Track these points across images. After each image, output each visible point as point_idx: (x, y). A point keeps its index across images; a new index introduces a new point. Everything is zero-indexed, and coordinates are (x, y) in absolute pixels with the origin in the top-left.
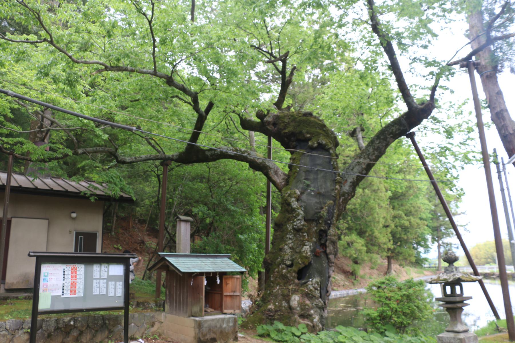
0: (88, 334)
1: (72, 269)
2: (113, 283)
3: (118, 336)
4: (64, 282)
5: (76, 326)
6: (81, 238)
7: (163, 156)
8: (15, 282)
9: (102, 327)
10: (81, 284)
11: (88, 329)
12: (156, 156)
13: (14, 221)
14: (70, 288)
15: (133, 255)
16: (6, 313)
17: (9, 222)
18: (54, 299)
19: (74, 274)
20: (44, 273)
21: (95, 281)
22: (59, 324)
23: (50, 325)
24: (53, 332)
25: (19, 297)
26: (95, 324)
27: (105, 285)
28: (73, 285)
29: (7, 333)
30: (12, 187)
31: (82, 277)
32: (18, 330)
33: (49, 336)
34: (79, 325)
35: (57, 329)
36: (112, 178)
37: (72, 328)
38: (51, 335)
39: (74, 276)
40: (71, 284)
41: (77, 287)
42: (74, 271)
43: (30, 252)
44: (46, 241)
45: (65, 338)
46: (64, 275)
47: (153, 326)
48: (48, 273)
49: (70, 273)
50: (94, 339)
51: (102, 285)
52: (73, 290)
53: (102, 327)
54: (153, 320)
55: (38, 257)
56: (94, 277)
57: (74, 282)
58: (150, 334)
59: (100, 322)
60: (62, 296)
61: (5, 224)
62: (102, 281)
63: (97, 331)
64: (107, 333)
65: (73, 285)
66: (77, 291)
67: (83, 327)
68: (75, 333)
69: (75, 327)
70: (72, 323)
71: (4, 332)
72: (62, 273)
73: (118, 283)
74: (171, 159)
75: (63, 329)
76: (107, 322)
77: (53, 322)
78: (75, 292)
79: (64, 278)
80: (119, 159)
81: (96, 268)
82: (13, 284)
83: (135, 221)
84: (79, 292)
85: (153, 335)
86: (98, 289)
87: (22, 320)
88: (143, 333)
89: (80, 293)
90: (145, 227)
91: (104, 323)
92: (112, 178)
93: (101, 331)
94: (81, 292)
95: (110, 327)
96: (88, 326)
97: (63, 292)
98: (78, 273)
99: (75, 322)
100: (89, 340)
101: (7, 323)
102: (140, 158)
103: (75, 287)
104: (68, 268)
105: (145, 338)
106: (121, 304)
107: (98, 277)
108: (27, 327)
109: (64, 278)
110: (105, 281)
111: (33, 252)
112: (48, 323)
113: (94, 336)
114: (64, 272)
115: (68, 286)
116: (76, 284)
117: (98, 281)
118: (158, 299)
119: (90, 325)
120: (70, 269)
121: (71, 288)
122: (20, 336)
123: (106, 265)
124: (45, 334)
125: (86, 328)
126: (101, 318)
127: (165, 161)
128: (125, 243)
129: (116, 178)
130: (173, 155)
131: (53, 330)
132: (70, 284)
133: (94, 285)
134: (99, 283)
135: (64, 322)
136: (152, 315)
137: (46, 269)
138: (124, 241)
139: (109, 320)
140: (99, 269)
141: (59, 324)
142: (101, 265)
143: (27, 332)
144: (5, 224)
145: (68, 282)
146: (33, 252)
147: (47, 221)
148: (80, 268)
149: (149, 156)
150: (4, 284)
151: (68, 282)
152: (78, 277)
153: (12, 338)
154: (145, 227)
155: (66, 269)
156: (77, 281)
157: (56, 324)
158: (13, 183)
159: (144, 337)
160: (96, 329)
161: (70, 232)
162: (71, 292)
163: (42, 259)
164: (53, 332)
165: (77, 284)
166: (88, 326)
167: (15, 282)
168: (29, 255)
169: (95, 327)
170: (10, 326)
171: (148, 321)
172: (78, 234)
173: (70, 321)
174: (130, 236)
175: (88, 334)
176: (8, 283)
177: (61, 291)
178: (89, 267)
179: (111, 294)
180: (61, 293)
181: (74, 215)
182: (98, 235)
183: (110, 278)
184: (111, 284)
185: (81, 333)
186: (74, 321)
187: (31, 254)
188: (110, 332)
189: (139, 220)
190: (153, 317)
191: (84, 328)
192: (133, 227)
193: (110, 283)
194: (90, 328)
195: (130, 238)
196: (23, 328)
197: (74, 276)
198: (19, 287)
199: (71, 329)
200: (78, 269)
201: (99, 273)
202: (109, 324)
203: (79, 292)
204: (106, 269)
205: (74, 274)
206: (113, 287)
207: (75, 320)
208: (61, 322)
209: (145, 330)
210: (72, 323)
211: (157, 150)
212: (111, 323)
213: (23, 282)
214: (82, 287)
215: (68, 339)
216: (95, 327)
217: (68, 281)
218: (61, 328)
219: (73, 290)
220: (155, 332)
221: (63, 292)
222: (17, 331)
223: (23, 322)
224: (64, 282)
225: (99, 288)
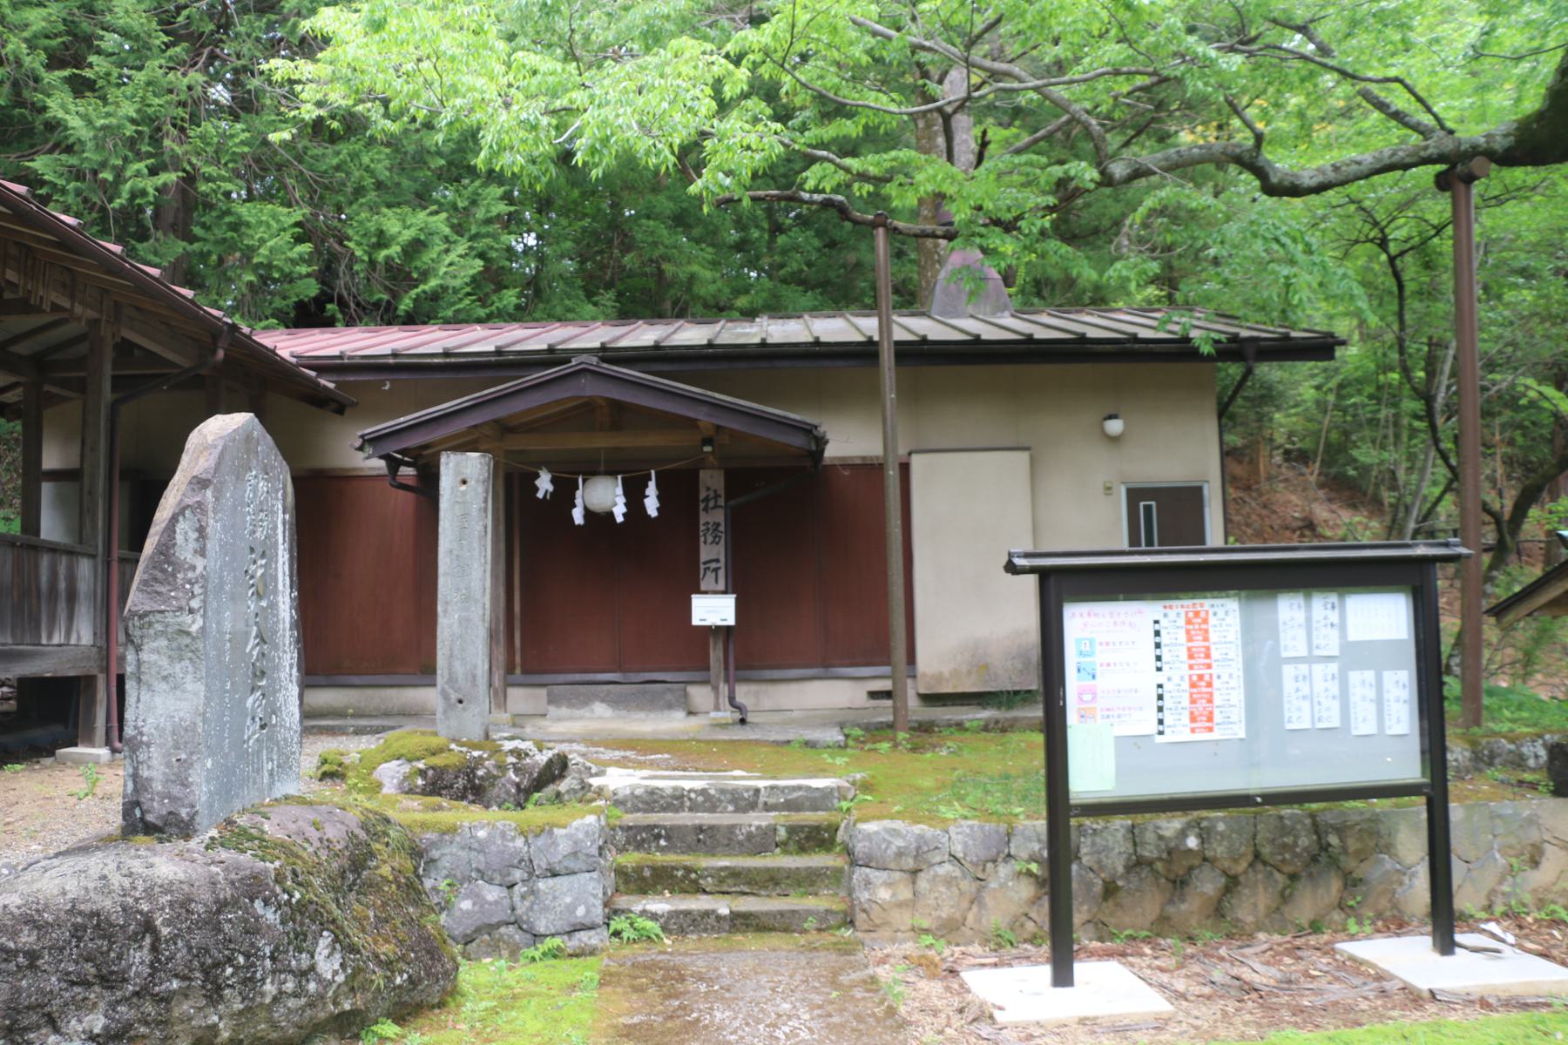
0: (1261, 889)
1: (1189, 622)
2: (1369, 675)
3: (1383, 903)
4: (1160, 678)
5: (1209, 854)
6: (1148, 509)
7: (1448, 145)
8: (946, 674)
9: (1314, 859)
10: (1233, 683)
11: (1260, 867)
12: (1418, 148)
13: (917, 462)
14: (1186, 702)
15: (1447, 545)
16: (941, 786)
17: (905, 469)
18: (1129, 746)
19: (1198, 643)
20: (1078, 641)
21: (1288, 671)
22: (1144, 843)
23: (1107, 849)
24: (1121, 877)
25: (967, 725)
26: (1284, 846)
27: (1335, 688)
28: (1201, 687)
29: (958, 873)
30: (897, 343)
31: (1235, 653)
32: (994, 861)
33: (1110, 890)
34: (1219, 850)
35: (1137, 864)
36: (1277, 240)
37: (1196, 862)
38: (1117, 888)
39: (1200, 655)
40: (1193, 685)
41: (1217, 700)
42: (1197, 628)
43: (1010, 555)
44: (1029, 526)
45: (1171, 901)
46: (1158, 645)
47: (1535, 863)
48: (1091, 642)
49: (1182, 636)
50: (1286, 909)
51: (1319, 685)
52: (1203, 717)
53: (1314, 859)
54: (1534, 835)
55: (1044, 574)
56: (1284, 654)
57: (1201, 677)
58: (1528, 898)
59: (1304, 841)
60: (1159, 739)
61: (892, 473)
62: (1318, 668)
63: (1293, 877)
64: (1335, 885)
65: (1201, 687)
66: (1217, 718)
67: (1236, 861)
68: (1208, 885)
69: (1205, 859)
70: (1192, 842)
71: (948, 867)
72: (1152, 640)
73: (1389, 677)
74: (1475, 152)
75: (1159, 866)
76: (1333, 840)
77: (1119, 835)
78: (1210, 719)
79: (1159, 658)
80: (1274, 180)
81: (1289, 610)
82: (939, 678)
83: (1271, 457)
84: (1228, 721)
85: (1541, 904)
86: (1306, 705)
87: (1003, 827)
88: (1493, 892)
89: (1232, 724)
90: (1312, 473)
91: (1325, 848)
92: (1277, 240)
93: (1310, 876)
94: (1234, 718)
95: (1349, 863)
96: (1257, 856)
97: (1161, 722)
98: (1213, 637)
99: (1203, 840)
100: (1267, 916)
101: (953, 836)
102: (1354, 167)
103: (1210, 701)
104: (1172, 614)
105: (1505, 915)
106: (1410, 769)
107: (1303, 652)
108: (1025, 855)
109: (1159, 658)
110: (1333, 668)
111: (1027, 555)
112: (1098, 840)
113: (1285, 898)
114: (1157, 633)
115: (1178, 697)
116: (1209, 685)
117: (1304, 668)
118: (1476, 729)
119: (1266, 851)
120: (1182, 621)
121: (1193, 701)
122: (1003, 886)
123: (1333, 598)
124: (1093, 884)
125: (1251, 865)
126: (1308, 821)
127: (1457, 169)
128: (1249, 531)
129: (1294, 240)
130: (1489, 136)
131: (1120, 869)
132: (1186, 685)
133: (1289, 685)
134: (1308, 678)
135: (1161, 838)
136: (1526, 813)
137: (1083, 622)
138: (1248, 525)
139: (1340, 830)
140: (1300, 616)
141: (1144, 843)
142: (1308, 597)
143: (1029, 873)
144: (892, 473)
145: (1176, 680)
146: (1027, 555)
147: (1025, 456)
148: (1221, 613)
149: (1387, 153)
150: (914, 677)
151: (1176, 680)
152: (1215, 654)
153: (979, 891)
154: (1312, 473)
155: (1164, 622)
156: (1215, 671)
157: (1129, 845)
158: (899, 335)
159: (1499, 909)
160: (1288, 869)
161: (1108, 489)
162: (1193, 719)
163: (1062, 584)
164: (1121, 877)
165: (1216, 683)
166: (1257, 856)
167: (946, 674)
168: (1011, 568)
169: (1284, 861)
170: (965, 845)
171: (1512, 840)
172: (1135, 495)
173: (1183, 834)
174: (1265, 506)
175: (1261, 889)
176: (924, 675)
177: (1154, 716)
178: (1260, 608)
179: (1364, 724)
180: (1153, 727)
181: (1114, 427)
182: (1206, 492)
183: (1355, 655)
184: (1362, 681)
185: (1232, 883)
186: (1200, 836)
187: (1019, 562)
188: (1351, 882)
189: (1287, 452)
190: (1531, 821)
191: (1243, 865)
192: (1269, 478)
193: (1354, 677)
194: (1265, 863)
195: (1264, 512)
196: (1009, 855)
197: (1200, 655)
198: (960, 690)
199: (1191, 869)
200: (1212, 620)
201: (1302, 633)
202: (1345, 850)
203: (1228, 721)
204: (1334, 617)
205: (1198, 643)
206: (1372, 694)
207: (1205, 836)
208: (1150, 836)
209: (1502, 880)
210: (1192, 842)
211: (1417, 128)
212: (1353, 844)
213: (969, 673)
214: (1238, 697)
215: (1184, 907)
216: (1284, 861)
217: (1178, 674)
218: (1150, 863)
219: (1203, 717)
220: (1547, 890)
221: (1161, 722)
222: (990, 865)
223: (1008, 835)
224: (1160, 678)
225: (1308, 700)
